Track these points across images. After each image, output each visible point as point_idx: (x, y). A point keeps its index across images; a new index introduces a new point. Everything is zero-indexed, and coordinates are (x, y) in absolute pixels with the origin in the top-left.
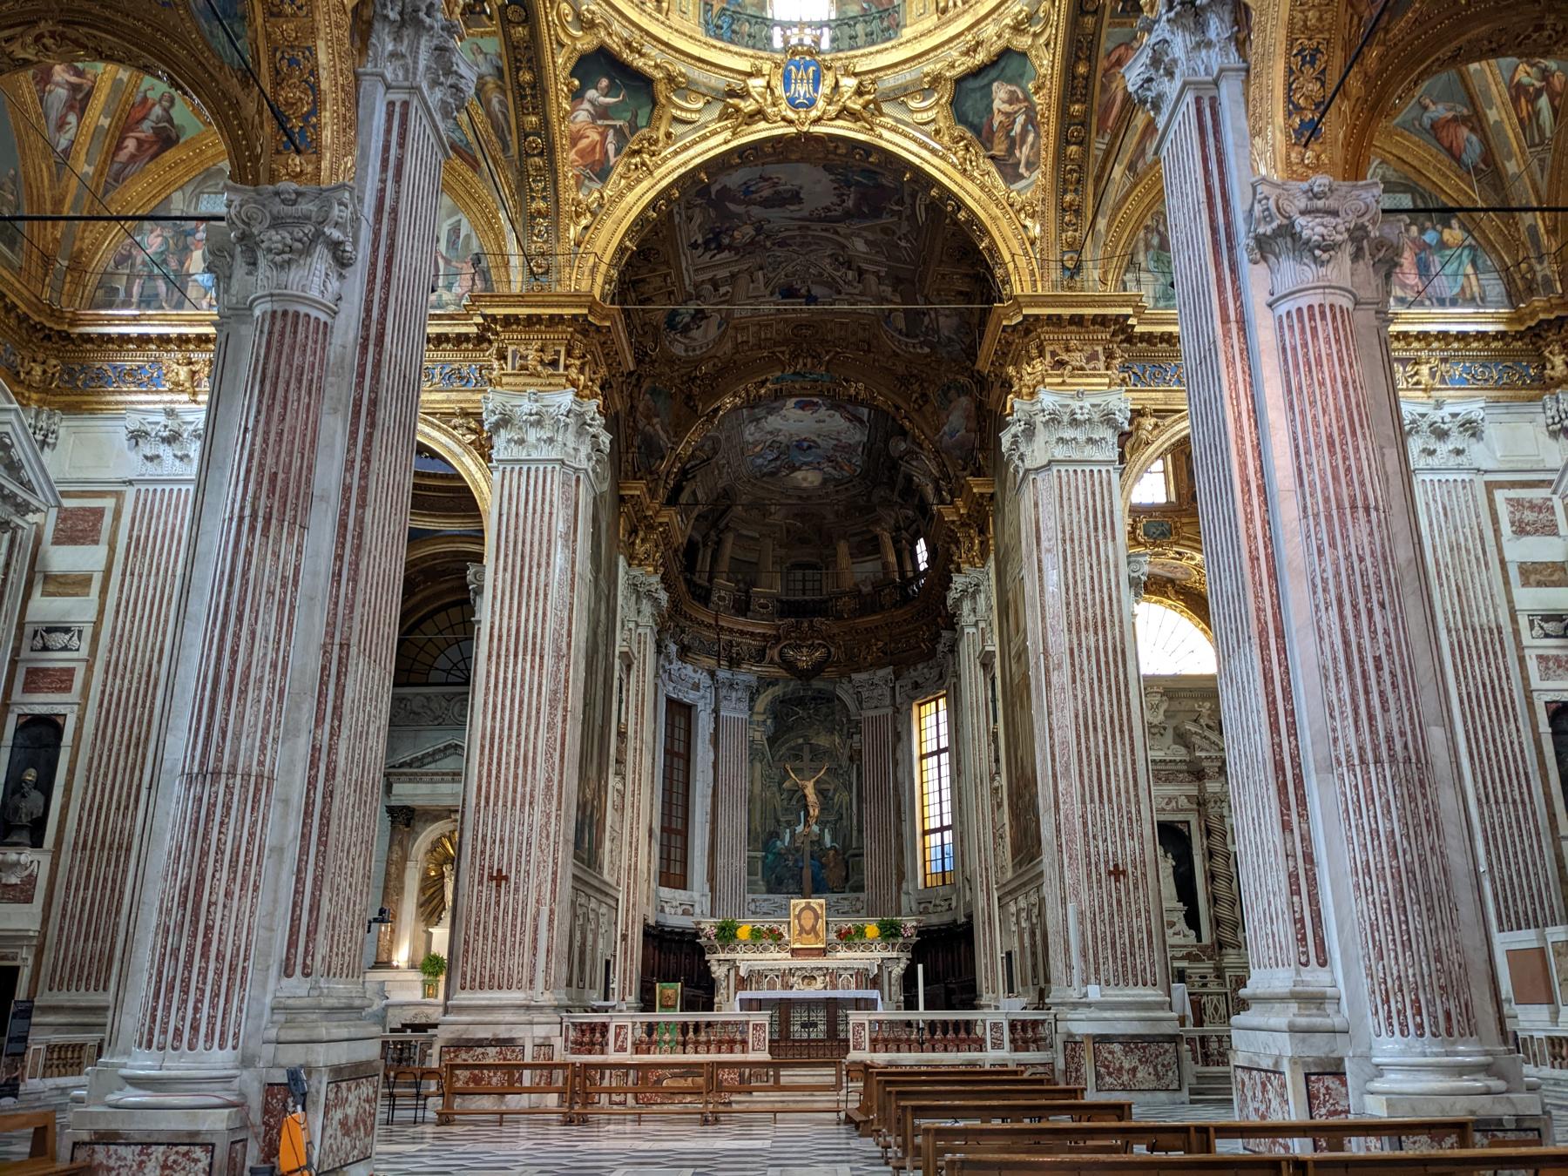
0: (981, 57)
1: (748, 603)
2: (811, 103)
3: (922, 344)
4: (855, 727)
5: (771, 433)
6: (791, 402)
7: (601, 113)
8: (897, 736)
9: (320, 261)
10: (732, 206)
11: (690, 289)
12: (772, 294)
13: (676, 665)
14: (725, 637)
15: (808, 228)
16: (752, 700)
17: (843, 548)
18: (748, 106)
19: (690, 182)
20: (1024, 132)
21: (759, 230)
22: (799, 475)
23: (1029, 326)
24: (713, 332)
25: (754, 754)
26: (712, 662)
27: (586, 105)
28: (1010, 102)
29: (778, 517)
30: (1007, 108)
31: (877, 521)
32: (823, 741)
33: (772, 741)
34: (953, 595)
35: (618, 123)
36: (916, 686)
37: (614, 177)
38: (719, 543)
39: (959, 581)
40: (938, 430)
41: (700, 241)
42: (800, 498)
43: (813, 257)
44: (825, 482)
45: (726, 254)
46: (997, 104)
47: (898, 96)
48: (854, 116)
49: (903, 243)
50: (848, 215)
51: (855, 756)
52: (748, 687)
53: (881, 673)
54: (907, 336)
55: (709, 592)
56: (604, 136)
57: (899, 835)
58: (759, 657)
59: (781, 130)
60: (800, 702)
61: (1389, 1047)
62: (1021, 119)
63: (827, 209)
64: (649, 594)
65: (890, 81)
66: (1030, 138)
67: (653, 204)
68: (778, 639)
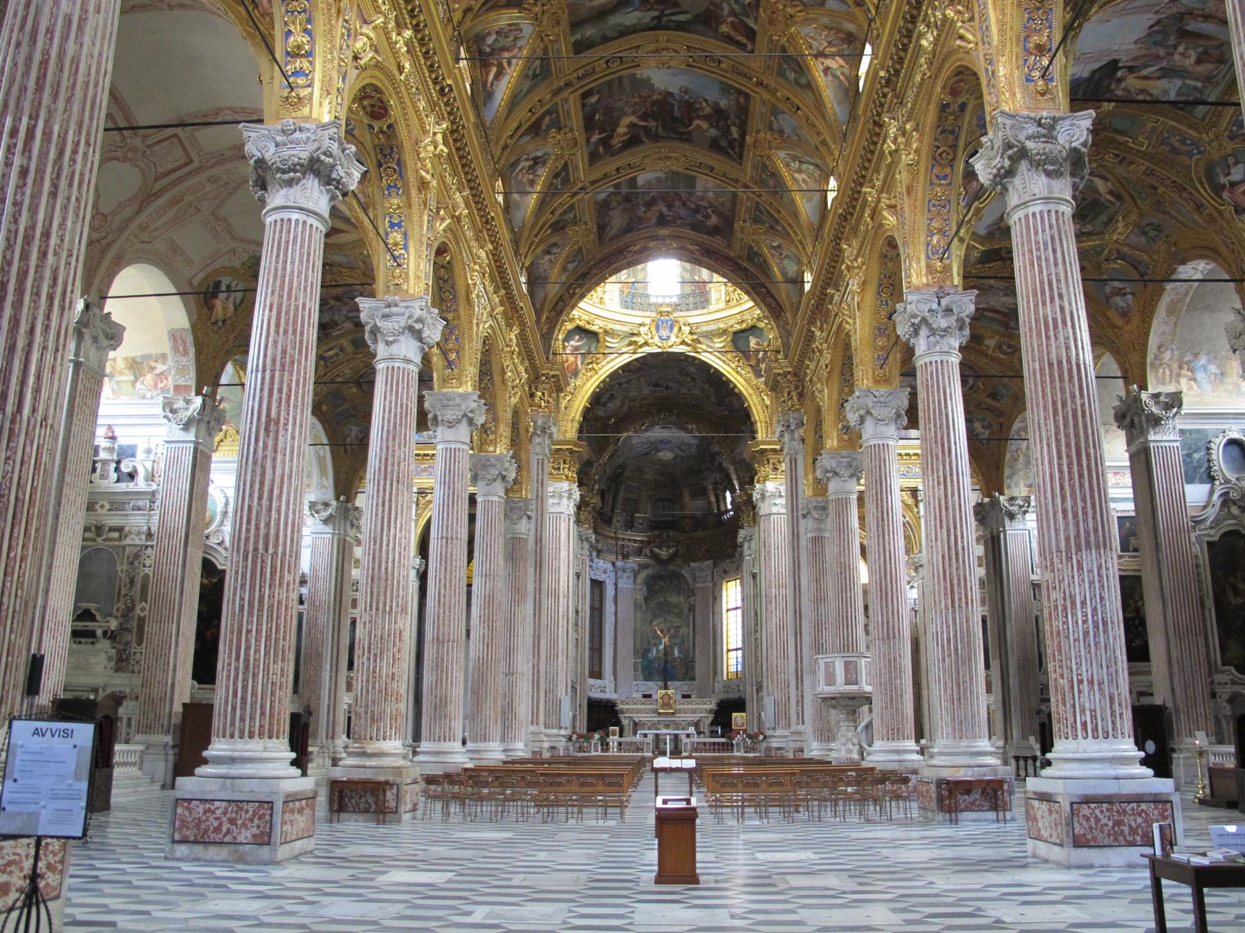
0: (744, 326)
1: (632, 523)
2: (669, 338)
4: (692, 592)
7: (576, 348)
8: (715, 598)
9: (525, 520)
13: (596, 560)
14: (620, 543)
16: (635, 576)
17: (686, 493)
18: (640, 340)
19: (614, 375)
22: (661, 454)
23: (763, 452)
24: (618, 402)
25: (637, 607)
26: (613, 558)
29: (649, 475)
31: (704, 479)
32: (674, 599)
33: (646, 599)
34: (740, 540)
36: (725, 572)
37: (580, 375)
38: (617, 490)
39: (742, 533)
40: (733, 451)
44: (676, 457)
47: (710, 335)
48: (688, 345)
51: (692, 609)
52: (633, 570)
53: (707, 563)
55: (611, 518)
57: (715, 652)
58: (639, 552)
59: (655, 350)
60: (661, 577)
61: (815, 745)
64: (587, 540)
65: (705, 329)
67: (598, 387)
68: (649, 543)
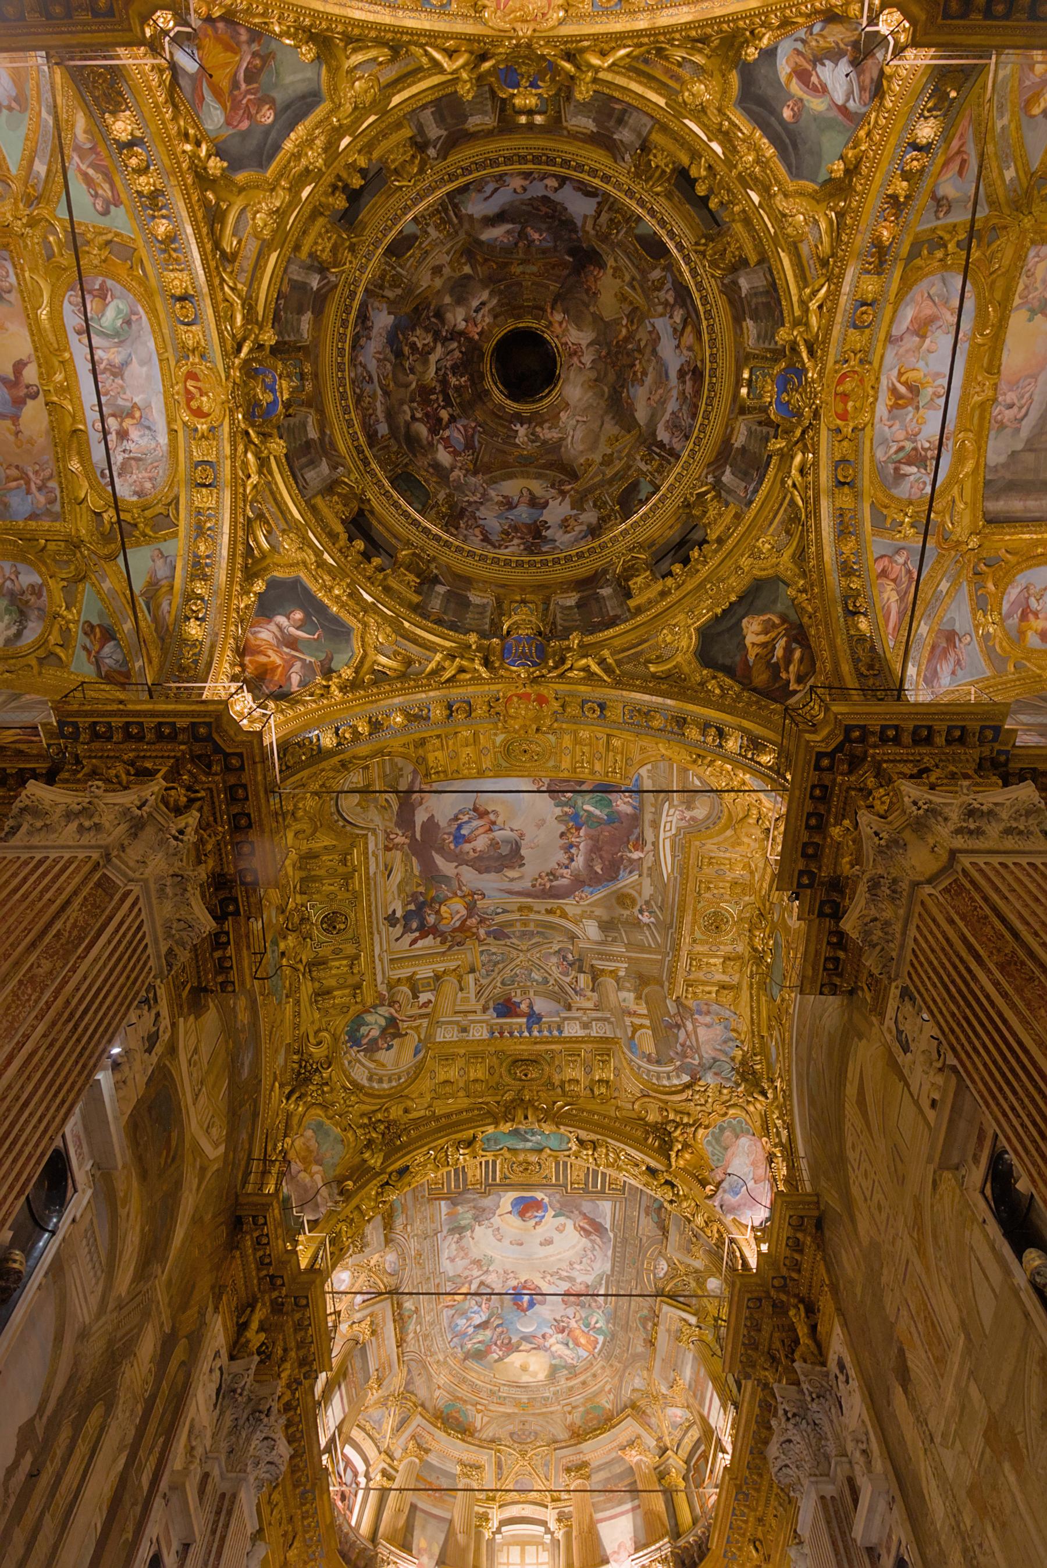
3: (680, 1070)
5: (478, 1263)
6: (509, 1197)
10: (439, 860)
11: (383, 989)
12: (485, 1009)
15: (530, 909)
20: (788, 651)
21: (471, 908)
27: (272, 627)
28: (766, 632)
30: (763, 639)
35: (308, 659)
41: (399, 914)
42: (517, 1403)
43: (534, 955)
45: (429, 941)
46: (750, 639)
49: (645, 918)
50: (578, 883)
54: (658, 1062)
56: (289, 665)
62: (782, 643)
63: (553, 875)
66: (797, 654)
